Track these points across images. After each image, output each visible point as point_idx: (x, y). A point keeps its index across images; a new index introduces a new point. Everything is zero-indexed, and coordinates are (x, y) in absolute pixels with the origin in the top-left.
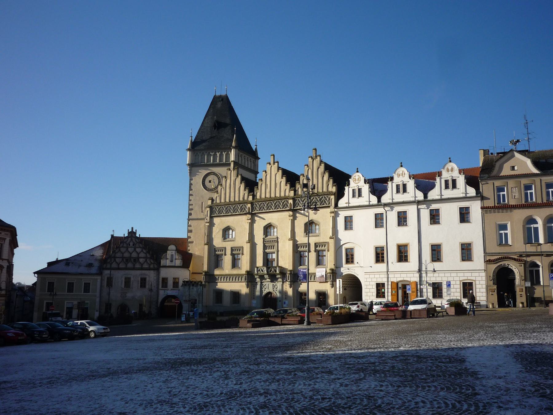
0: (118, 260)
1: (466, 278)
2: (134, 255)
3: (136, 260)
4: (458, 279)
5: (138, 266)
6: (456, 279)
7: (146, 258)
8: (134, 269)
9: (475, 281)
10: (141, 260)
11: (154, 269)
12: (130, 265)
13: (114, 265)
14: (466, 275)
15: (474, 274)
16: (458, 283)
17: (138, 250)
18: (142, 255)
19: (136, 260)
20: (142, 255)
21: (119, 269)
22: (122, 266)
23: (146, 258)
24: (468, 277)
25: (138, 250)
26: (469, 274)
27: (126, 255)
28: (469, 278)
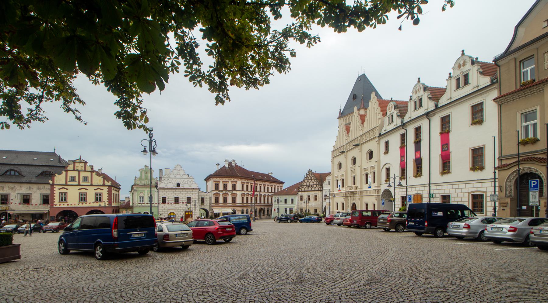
0: (305, 187)
1: (475, 189)
2: (311, 183)
3: (312, 186)
4: (465, 190)
5: (313, 189)
6: (464, 190)
7: (317, 185)
8: (311, 191)
9: (486, 192)
10: (315, 186)
11: (320, 190)
12: (310, 189)
13: (303, 190)
14: (475, 185)
15: (484, 185)
16: (466, 195)
17: (313, 181)
18: (315, 183)
19: (312, 186)
20: (315, 183)
21: (305, 191)
22: (306, 189)
23: (317, 185)
24: (478, 188)
25: (313, 181)
26: (479, 185)
27: (308, 184)
28: (479, 189)
